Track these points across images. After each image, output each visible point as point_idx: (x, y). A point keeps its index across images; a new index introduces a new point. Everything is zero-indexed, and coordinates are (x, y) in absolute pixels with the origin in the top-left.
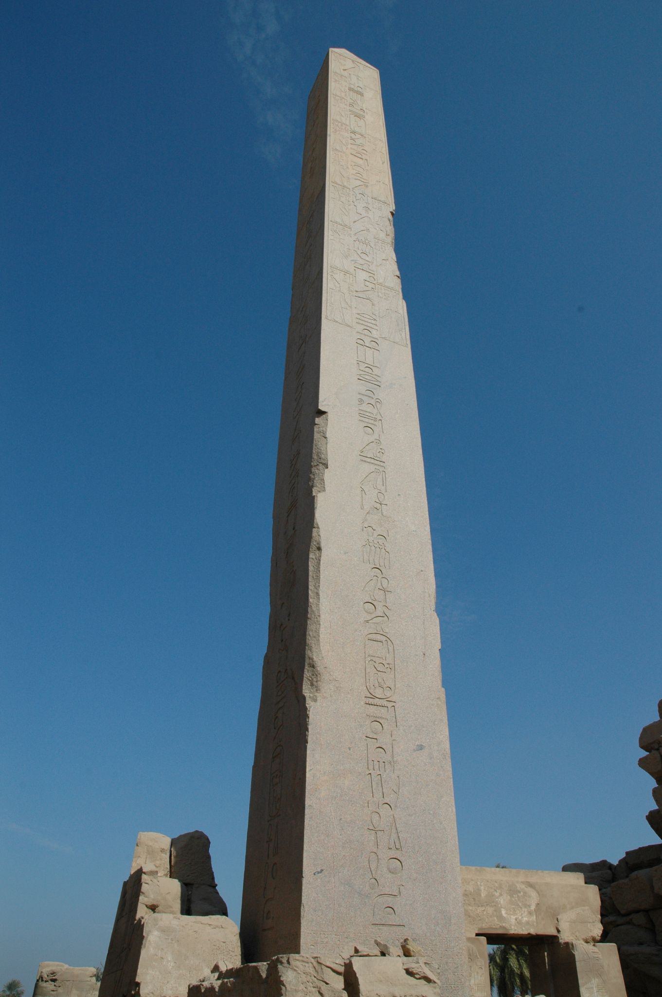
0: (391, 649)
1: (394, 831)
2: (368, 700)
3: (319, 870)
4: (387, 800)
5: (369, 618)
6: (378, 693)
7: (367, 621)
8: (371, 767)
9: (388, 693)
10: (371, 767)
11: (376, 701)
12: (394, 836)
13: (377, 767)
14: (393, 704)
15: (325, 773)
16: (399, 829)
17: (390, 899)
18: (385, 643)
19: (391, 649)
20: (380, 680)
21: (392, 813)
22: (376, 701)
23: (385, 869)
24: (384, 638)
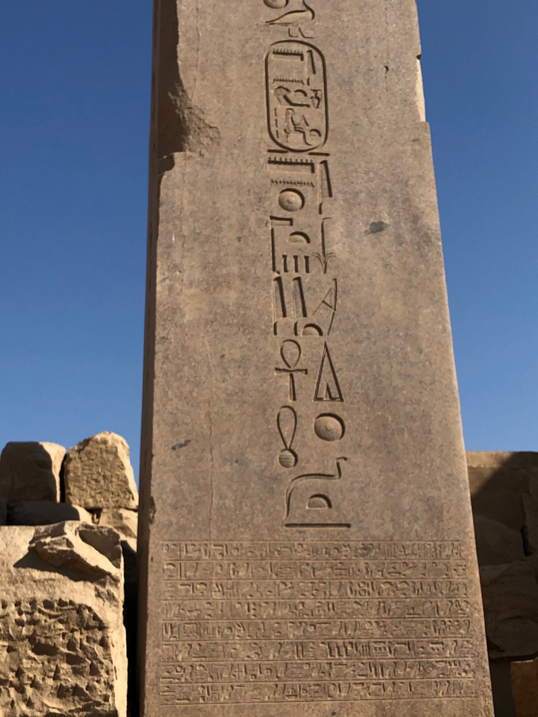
0: (318, 63)
1: (327, 368)
2: (273, 156)
3: (182, 441)
4: (311, 318)
5: (273, 14)
6: (295, 141)
7: (271, 22)
8: (280, 266)
9: (314, 141)
10: (280, 266)
11: (290, 156)
12: (327, 377)
13: (291, 266)
14: (323, 158)
15: (191, 284)
16: (336, 367)
17: (319, 481)
18: (306, 56)
19: (318, 63)
20: (297, 119)
21: (323, 339)
22: (290, 156)
23: (311, 433)
24: (304, 49)
